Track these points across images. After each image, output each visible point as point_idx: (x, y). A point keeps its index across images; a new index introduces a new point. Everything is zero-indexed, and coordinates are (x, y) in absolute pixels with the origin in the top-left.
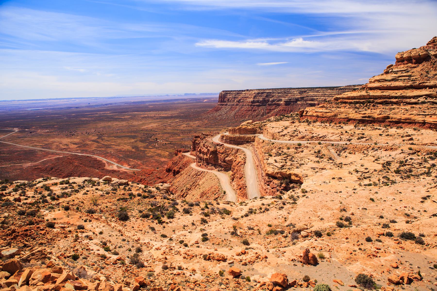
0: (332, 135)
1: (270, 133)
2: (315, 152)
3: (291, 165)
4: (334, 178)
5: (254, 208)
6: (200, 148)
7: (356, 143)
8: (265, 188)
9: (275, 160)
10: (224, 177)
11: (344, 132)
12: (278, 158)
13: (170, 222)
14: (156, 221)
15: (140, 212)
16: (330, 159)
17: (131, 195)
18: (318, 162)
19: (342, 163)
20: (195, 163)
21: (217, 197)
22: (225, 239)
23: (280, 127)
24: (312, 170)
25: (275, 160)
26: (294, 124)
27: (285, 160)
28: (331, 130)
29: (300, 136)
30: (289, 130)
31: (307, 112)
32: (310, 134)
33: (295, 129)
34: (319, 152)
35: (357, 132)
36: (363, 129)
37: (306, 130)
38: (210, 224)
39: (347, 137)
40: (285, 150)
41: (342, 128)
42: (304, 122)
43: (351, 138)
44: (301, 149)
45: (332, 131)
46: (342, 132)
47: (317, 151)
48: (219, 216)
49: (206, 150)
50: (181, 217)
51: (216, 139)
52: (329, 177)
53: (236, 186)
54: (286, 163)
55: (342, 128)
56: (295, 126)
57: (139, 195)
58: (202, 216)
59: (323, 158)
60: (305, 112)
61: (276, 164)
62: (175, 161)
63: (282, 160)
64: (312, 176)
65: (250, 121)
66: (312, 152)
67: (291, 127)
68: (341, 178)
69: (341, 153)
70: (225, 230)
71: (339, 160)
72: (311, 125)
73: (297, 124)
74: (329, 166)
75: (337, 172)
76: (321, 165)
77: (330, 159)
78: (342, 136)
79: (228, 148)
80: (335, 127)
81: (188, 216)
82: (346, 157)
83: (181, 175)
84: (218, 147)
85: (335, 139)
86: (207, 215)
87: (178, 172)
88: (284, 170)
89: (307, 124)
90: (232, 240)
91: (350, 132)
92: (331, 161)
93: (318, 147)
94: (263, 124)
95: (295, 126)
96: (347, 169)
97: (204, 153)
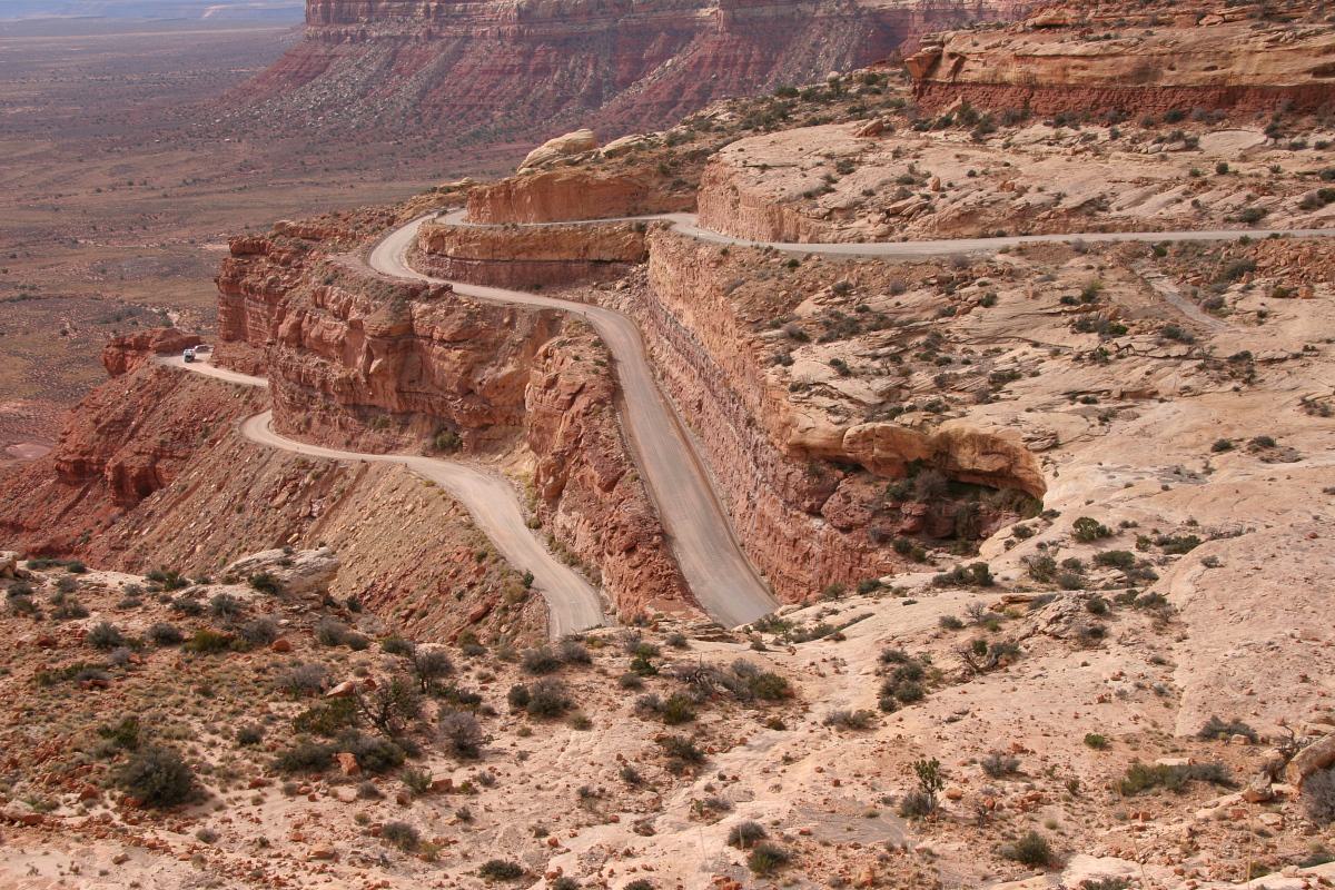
0: (1138, 191)
1: (755, 201)
2: (1066, 301)
3: (941, 383)
4: (1222, 447)
5: (911, 651)
6: (291, 318)
7: (1300, 234)
8: (788, 531)
9: (834, 363)
10: (490, 494)
11: (1210, 172)
12: (848, 349)
13: (488, 782)
14: (394, 787)
15: (248, 739)
16: (1173, 334)
17: (106, 640)
18: (1099, 357)
19: (1246, 355)
20: (267, 416)
21: (479, 608)
22: (891, 849)
23: (808, 162)
24: (1079, 405)
25: (834, 363)
26: (890, 144)
27: (896, 358)
28: (1125, 167)
29: (945, 207)
30: (867, 176)
31: (960, 60)
32: (1006, 195)
33: (900, 169)
34: (1090, 296)
35: (1293, 164)
36: (1321, 146)
37: (972, 174)
38: (721, 762)
39: (1237, 199)
40: (878, 302)
41: (1191, 145)
42: (946, 123)
43: (1263, 201)
44: (974, 288)
45: (1134, 170)
46: (1195, 174)
47: (1076, 294)
48: (744, 721)
49: (343, 327)
50: (525, 744)
51: (393, 257)
52: (1191, 439)
53: (583, 541)
54: (907, 373)
55: (1191, 145)
56: (897, 154)
57: (166, 638)
58: (652, 727)
59: (1121, 331)
60: (947, 65)
61: (845, 386)
62: (120, 409)
63: (875, 357)
64: (1088, 438)
65: (581, 135)
66: (1049, 301)
67: (871, 157)
68: (1264, 444)
69: (1228, 297)
70: (848, 792)
71: (1227, 339)
72: (997, 143)
73: (904, 138)
74: (1170, 380)
75: (1222, 405)
76: (1129, 374)
77: (1173, 334)
78: (1203, 198)
79: (487, 310)
80: (1150, 145)
81: (563, 732)
82: (1262, 315)
83: (186, 492)
84: (418, 307)
85: (1166, 213)
86: (675, 714)
87: (147, 483)
88: (907, 419)
89: (967, 136)
90: (928, 843)
91: (1243, 168)
92: (1180, 349)
93: (1076, 273)
94: (680, 149)
95: (897, 154)
96: (1287, 384)
97: (321, 347)
